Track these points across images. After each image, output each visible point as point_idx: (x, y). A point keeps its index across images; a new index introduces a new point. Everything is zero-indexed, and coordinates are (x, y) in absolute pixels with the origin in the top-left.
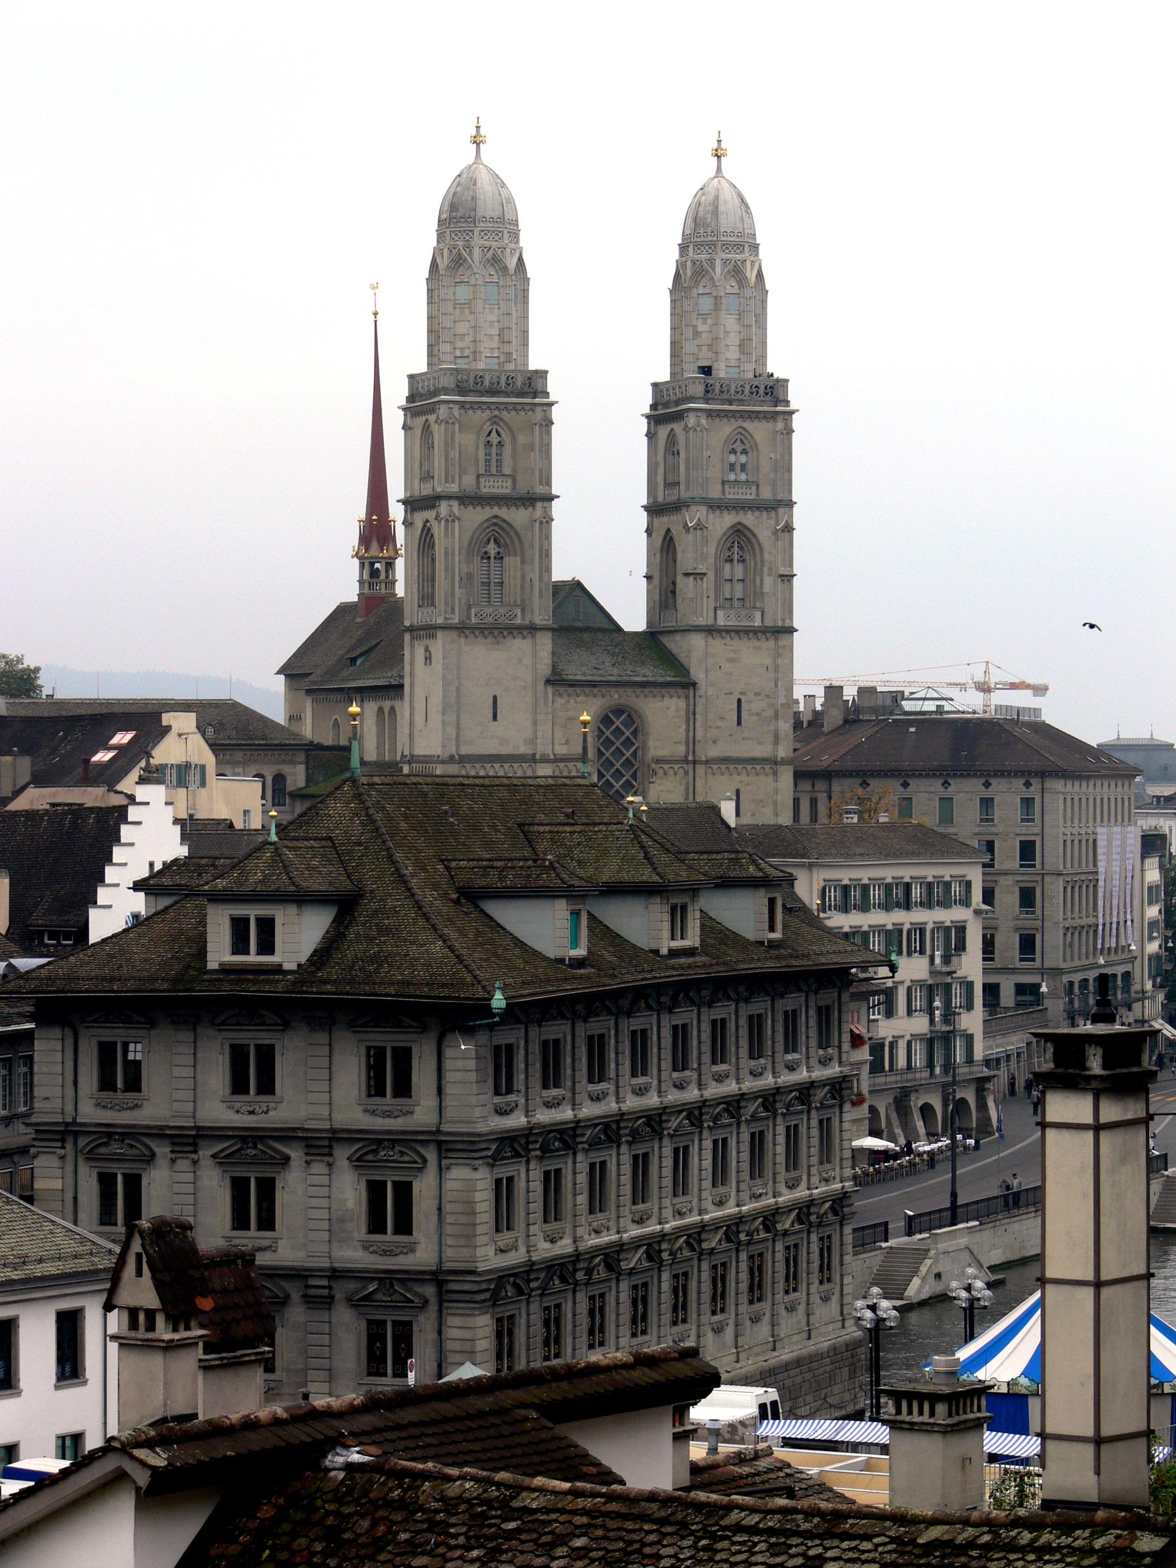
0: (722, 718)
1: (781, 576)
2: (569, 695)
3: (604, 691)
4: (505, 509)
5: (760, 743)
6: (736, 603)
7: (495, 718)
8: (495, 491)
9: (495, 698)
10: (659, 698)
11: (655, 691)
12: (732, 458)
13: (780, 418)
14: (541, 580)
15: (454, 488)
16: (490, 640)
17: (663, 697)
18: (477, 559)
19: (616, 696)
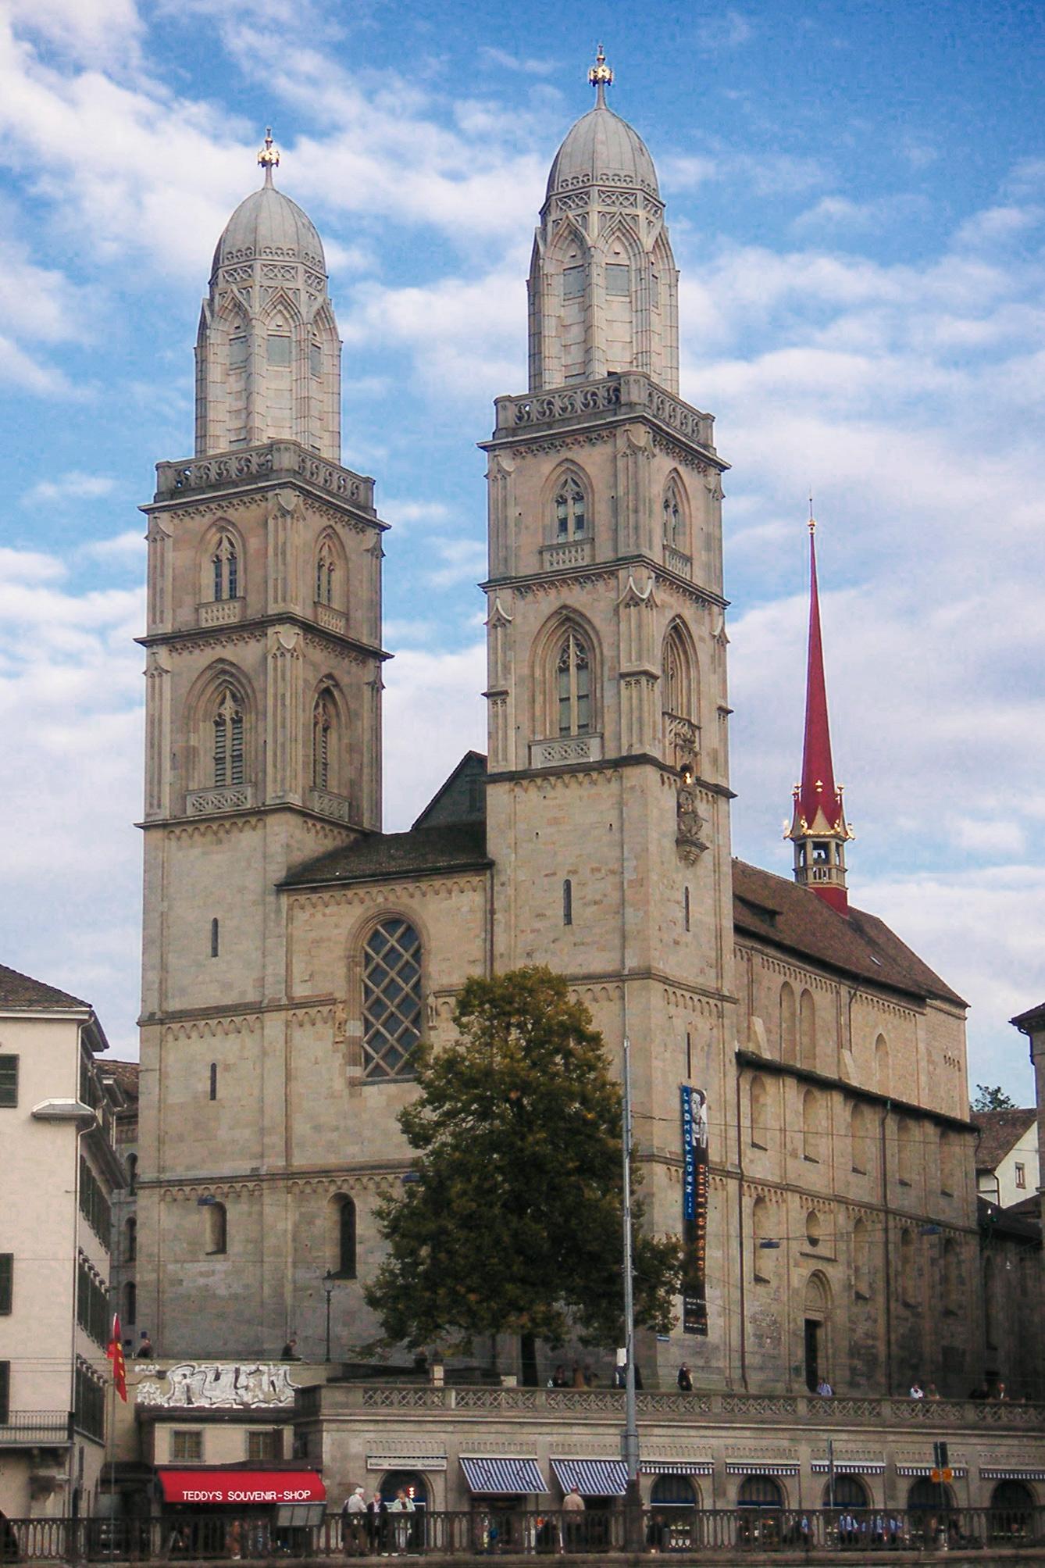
0: (538, 916)
1: (623, 676)
2: (314, 906)
3: (361, 892)
4: (230, 646)
5: (602, 949)
6: (574, 731)
7: (215, 954)
8: (221, 622)
9: (215, 921)
10: (443, 894)
11: (437, 883)
12: (561, 512)
13: (619, 431)
14: (275, 742)
15: (167, 628)
16: (210, 837)
17: (450, 892)
18: (207, 730)
19: (380, 899)
